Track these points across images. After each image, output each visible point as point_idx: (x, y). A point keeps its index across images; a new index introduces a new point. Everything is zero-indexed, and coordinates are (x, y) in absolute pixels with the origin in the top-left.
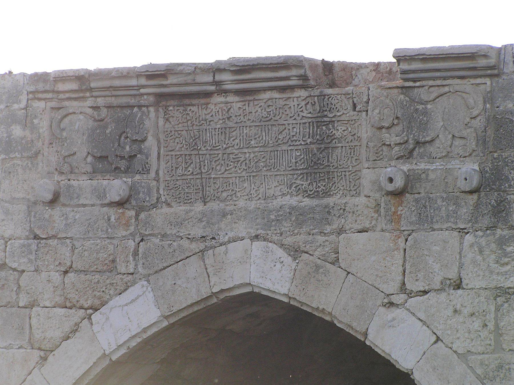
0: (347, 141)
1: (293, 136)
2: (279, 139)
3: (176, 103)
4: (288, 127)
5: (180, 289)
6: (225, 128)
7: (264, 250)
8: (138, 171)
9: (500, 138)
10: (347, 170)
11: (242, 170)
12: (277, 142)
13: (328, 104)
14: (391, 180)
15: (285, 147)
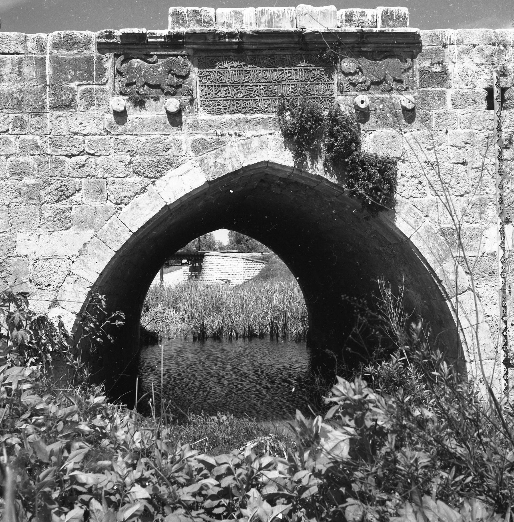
1: (289, 77)
5: (219, 165)
14: (362, 102)
15: (284, 83)
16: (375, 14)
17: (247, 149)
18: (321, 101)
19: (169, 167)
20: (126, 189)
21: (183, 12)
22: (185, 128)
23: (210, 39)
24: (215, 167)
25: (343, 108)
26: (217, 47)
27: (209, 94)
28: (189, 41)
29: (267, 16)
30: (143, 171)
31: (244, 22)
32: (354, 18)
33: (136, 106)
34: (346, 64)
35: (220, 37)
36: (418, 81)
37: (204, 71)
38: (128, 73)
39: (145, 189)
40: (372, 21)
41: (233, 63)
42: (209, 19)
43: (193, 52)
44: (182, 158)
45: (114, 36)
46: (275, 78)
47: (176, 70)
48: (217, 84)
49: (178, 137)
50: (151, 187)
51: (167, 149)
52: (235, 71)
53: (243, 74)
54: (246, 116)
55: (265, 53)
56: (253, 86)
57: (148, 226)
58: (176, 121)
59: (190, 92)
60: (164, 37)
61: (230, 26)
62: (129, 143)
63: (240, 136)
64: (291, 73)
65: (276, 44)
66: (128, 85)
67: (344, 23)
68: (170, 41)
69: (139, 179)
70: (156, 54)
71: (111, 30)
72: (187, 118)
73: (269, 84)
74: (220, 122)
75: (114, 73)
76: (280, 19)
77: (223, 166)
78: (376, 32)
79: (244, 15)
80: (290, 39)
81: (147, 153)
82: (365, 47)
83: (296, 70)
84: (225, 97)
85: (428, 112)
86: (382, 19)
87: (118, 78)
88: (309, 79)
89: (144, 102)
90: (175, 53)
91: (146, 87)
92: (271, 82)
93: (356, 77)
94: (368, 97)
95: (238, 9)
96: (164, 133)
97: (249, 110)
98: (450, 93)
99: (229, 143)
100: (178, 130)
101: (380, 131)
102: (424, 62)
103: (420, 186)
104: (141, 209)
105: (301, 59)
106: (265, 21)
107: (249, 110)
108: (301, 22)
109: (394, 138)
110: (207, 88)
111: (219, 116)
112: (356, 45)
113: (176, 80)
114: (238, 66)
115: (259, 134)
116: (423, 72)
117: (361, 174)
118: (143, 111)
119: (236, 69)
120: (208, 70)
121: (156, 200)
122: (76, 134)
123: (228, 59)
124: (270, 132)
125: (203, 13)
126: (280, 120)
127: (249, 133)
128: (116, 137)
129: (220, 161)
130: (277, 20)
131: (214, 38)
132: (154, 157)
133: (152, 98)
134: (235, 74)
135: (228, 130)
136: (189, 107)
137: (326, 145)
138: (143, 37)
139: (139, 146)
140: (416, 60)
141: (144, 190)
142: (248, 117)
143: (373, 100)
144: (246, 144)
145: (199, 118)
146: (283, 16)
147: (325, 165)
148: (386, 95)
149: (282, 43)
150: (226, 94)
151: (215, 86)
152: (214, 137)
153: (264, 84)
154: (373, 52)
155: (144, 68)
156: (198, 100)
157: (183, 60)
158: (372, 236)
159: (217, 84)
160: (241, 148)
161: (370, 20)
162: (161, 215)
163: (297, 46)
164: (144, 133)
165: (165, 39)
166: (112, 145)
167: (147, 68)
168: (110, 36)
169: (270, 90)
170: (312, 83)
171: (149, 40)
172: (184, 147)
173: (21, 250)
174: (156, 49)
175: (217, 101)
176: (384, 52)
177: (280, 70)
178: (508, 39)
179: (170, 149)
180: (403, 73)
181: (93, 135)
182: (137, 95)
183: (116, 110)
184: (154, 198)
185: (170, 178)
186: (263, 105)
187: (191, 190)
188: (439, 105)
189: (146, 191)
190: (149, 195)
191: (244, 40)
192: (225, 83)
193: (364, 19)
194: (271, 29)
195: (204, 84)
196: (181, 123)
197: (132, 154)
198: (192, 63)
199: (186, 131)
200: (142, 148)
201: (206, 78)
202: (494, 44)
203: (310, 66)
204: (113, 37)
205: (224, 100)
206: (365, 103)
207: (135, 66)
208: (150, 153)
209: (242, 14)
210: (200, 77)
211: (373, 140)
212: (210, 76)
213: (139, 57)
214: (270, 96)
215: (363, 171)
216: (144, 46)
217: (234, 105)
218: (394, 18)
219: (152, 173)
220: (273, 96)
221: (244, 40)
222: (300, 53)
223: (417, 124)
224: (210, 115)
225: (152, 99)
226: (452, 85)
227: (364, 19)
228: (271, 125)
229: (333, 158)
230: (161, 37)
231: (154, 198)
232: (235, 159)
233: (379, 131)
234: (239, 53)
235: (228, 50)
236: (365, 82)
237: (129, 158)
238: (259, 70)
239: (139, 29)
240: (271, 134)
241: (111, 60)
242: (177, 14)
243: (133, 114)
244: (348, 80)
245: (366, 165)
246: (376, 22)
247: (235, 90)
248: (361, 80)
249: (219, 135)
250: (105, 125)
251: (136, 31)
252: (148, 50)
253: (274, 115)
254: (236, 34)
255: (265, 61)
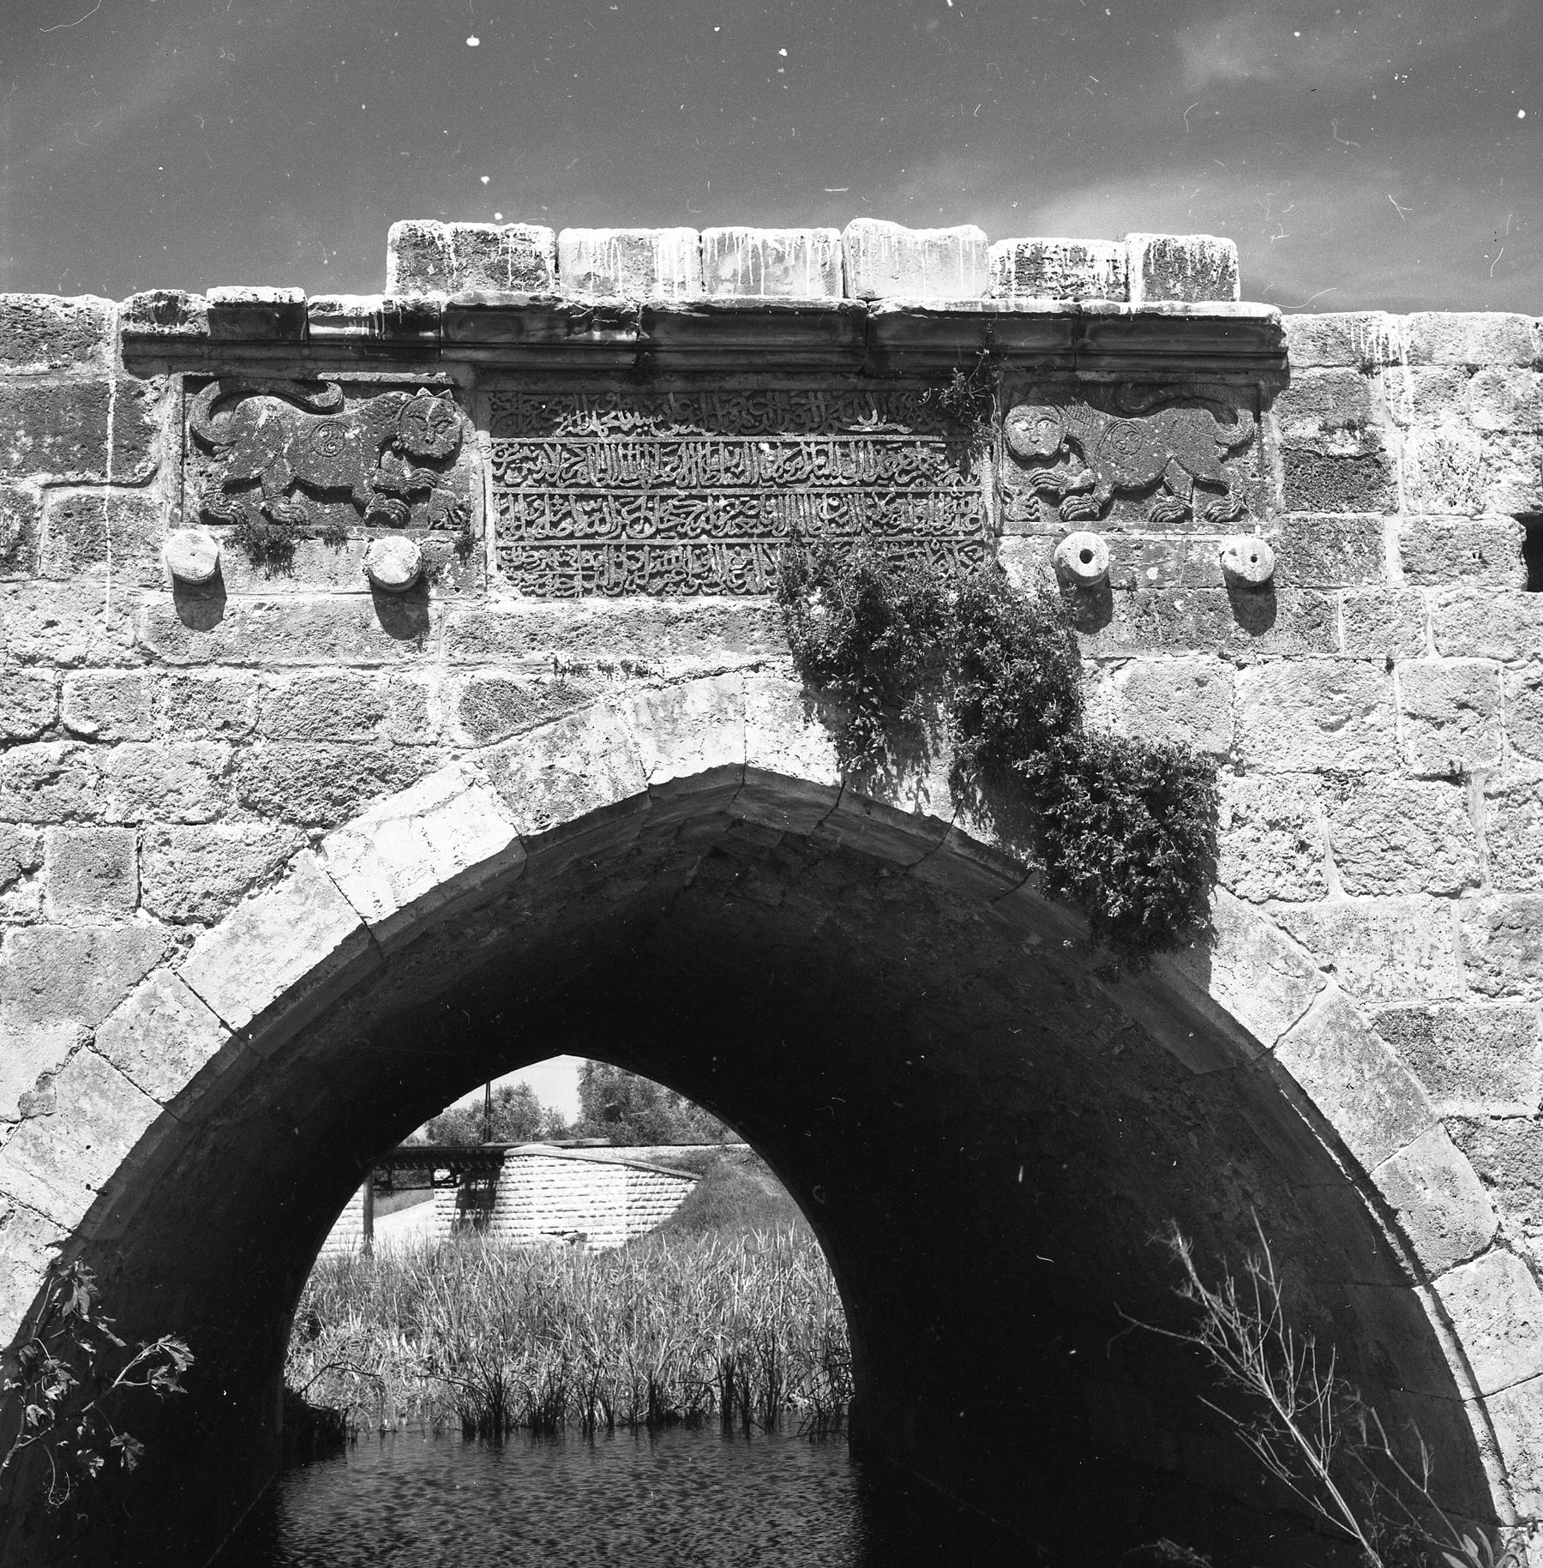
0: (947, 481)
1: (820, 467)
2: (786, 471)
3: (521, 388)
4: (805, 449)
5: (565, 778)
6: (651, 445)
7: (776, 695)
8: (435, 523)
9: (1298, 488)
10: (955, 538)
11: (699, 531)
12: (781, 477)
13: (897, 408)
14: (1086, 556)
15: (800, 489)
16: (1121, 258)
17: (667, 723)
18: (934, 552)
19: (376, 784)
20: (211, 864)
21: (441, 237)
22: (437, 644)
23: (537, 331)
24: (550, 784)
25: (1015, 576)
26: (560, 360)
27: (530, 524)
28: (459, 335)
29: (739, 255)
30: (276, 799)
31: (659, 275)
32: (1048, 269)
33: (257, 561)
34: (1024, 425)
35: (571, 325)
36: (1279, 487)
37: (511, 445)
38: (232, 444)
39: (285, 865)
40: (1112, 279)
41: (616, 418)
42: (532, 262)
43: (472, 376)
44: (426, 753)
45: (185, 314)
46: (770, 472)
47: (409, 439)
48: (558, 491)
49: (412, 676)
50: (306, 861)
51: (369, 718)
52: (625, 446)
53: (652, 456)
54: (665, 605)
55: (731, 383)
56: (690, 497)
57: (291, 1006)
58: (408, 618)
59: (460, 516)
60: (369, 320)
61: (605, 286)
62: (227, 697)
63: (641, 673)
64: (826, 454)
65: (772, 353)
66: (234, 487)
67: (1014, 285)
68: (390, 335)
69: (260, 828)
70: (338, 382)
71: (174, 292)
73: (748, 491)
74: (567, 622)
75: (183, 446)
76: (786, 270)
77: (578, 781)
78: (1128, 316)
79: (660, 250)
80: (824, 336)
81: (293, 734)
82: (1088, 369)
83: (845, 445)
84: (586, 536)
85: (1318, 593)
86: (1146, 275)
87: (195, 465)
88: (892, 478)
89: (291, 550)
90: (408, 376)
91: (298, 496)
92: (755, 486)
93: (1058, 470)
94: (1107, 541)
95: (636, 233)
96: (361, 660)
97: (677, 584)
98: (1394, 530)
99: (601, 698)
100: (413, 650)
101: (1151, 659)
102: (1298, 424)
103: (1302, 860)
104: (264, 940)
105: (862, 408)
106: (735, 274)
107: (677, 584)
108: (861, 278)
109: (1201, 683)
110: (522, 505)
111: (565, 604)
112: (1058, 361)
113: (408, 474)
114: (635, 427)
115: (714, 665)
116: (1296, 456)
117: (1089, 813)
118: (282, 583)
119: (630, 439)
120: (528, 441)
121: (325, 906)
122: (31, 660)
123: (602, 404)
124: (753, 660)
125: (512, 243)
126: (787, 617)
127: (676, 666)
128: (182, 673)
129: (569, 763)
130: (778, 270)
131: (551, 328)
132: (320, 746)
133: (318, 533)
134: (625, 457)
135: (597, 652)
136: (454, 570)
137: (955, 709)
138: (293, 314)
139: (266, 708)
140: (1272, 417)
141: (280, 868)
142: (673, 606)
143: (1122, 550)
144: (664, 703)
145: (493, 608)
146: (797, 258)
147: (955, 781)
148: (1174, 534)
149: (795, 348)
150: (591, 525)
151: (552, 497)
152: (548, 678)
153: (730, 491)
154: (1118, 384)
155: (295, 429)
156: (490, 545)
157: (435, 402)
158: (1117, 1051)
159: (558, 491)
160: (645, 718)
161: (1103, 277)
162: (343, 963)
163: (849, 361)
164: (284, 661)
165: (372, 327)
166: (166, 702)
167: (304, 427)
168: (171, 311)
169: (752, 512)
170: (903, 489)
171: (315, 330)
172: (433, 711)
174: (338, 364)
175: (558, 548)
176: (1154, 386)
177: (785, 445)
179: (380, 717)
180: (1223, 459)
181: (93, 665)
182: (262, 524)
183: (181, 573)
184: (317, 902)
185: (379, 824)
186: (724, 563)
187: (459, 870)
188: (1359, 573)
189: (286, 872)
190: (299, 890)
191: (659, 334)
192: (590, 485)
193: (1082, 272)
194: (756, 297)
195: (509, 490)
196: (425, 625)
197: (237, 736)
198: (471, 415)
199: (442, 655)
200: (275, 715)
201: (520, 469)
203: (896, 432)
204: (184, 317)
205: (584, 547)
206: (1094, 560)
207: (261, 422)
208: (307, 733)
209: (651, 248)
210: (498, 465)
211: (1127, 692)
212: (534, 460)
213: (279, 387)
214: (751, 536)
215: (1094, 800)
216: (292, 353)
217: (619, 565)
218: (1189, 272)
219: (312, 808)
220: (761, 535)
221: (659, 334)
222: (860, 385)
223: (1279, 639)
224: (533, 598)
225: (321, 540)
226: (1402, 502)
227: (1082, 272)
228: (757, 635)
229: (982, 757)
230: (358, 320)
231: (317, 902)
232: (624, 758)
233: (1146, 662)
234: (638, 383)
235: (602, 373)
236: (1091, 489)
237: (225, 749)
238: (712, 444)
239: (279, 291)
240: (755, 668)
241: (172, 399)
242: (416, 245)
244: (1033, 482)
245: (1101, 778)
246: (1126, 285)
247: (624, 511)
248: (1076, 482)
249: (564, 670)
250: (139, 630)
251: (267, 294)
252: (310, 365)
253: (764, 603)
254: (630, 316)
255: (735, 411)
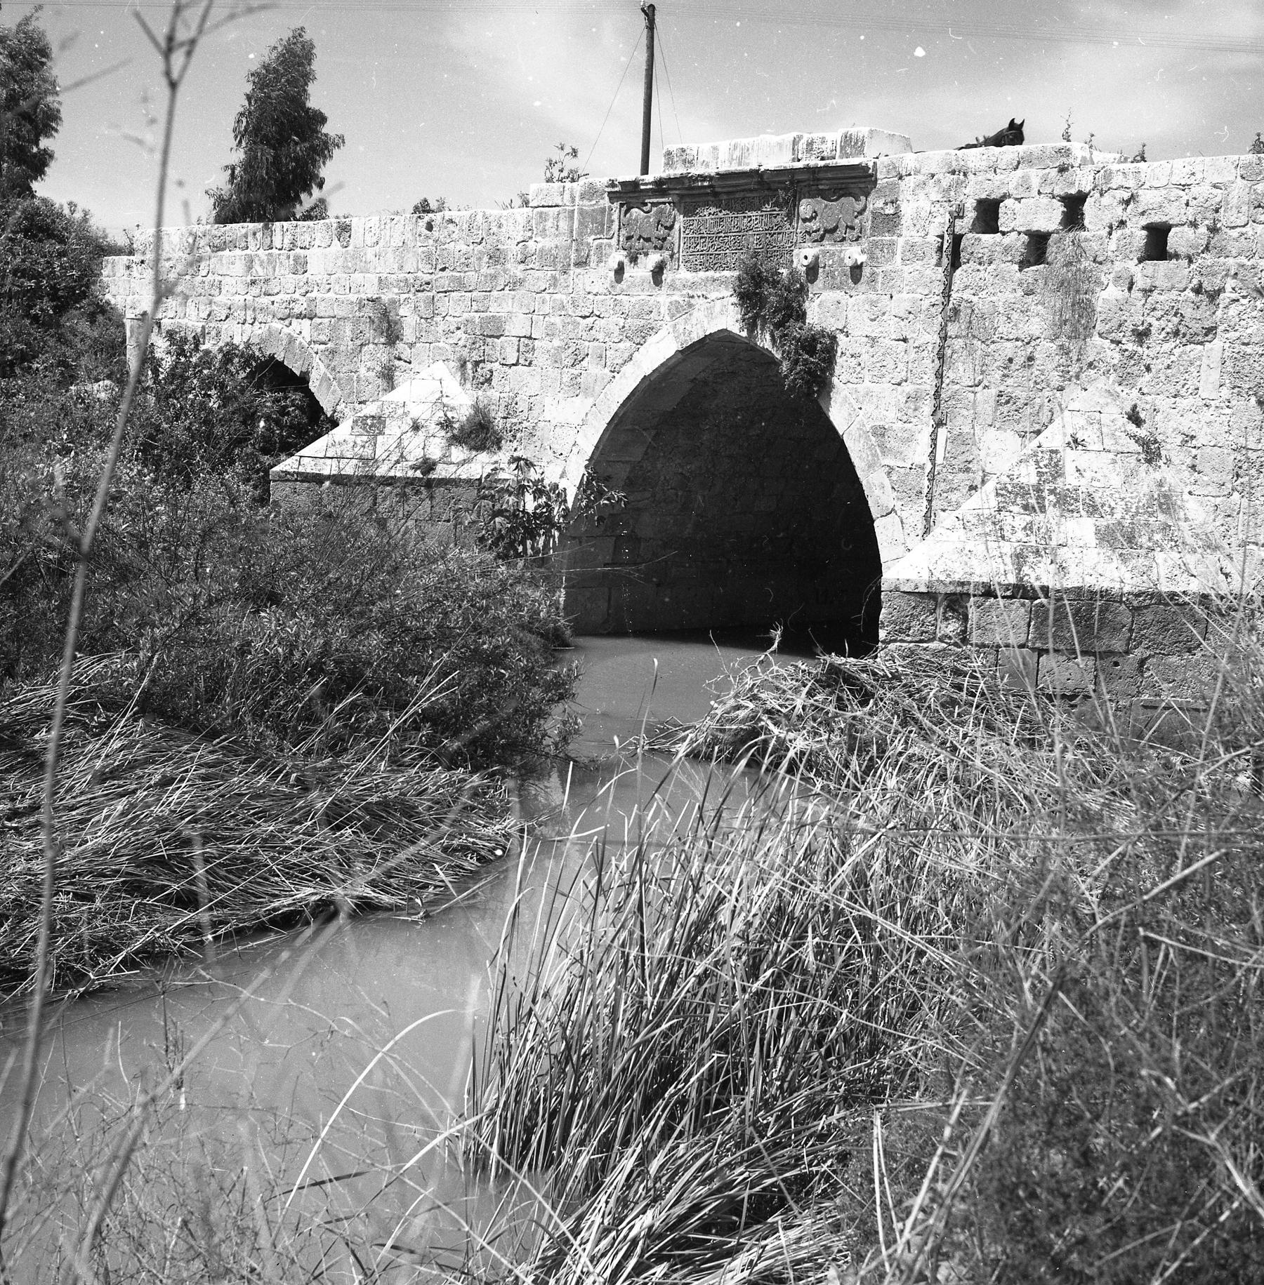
17: (710, 314)
55: (737, 196)
69: (628, 344)
72: (667, 276)
98: (901, 242)
103: (859, 369)
116: (875, 215)
127: (713, 296)
148: (837, 247)
173: (547, 416)
178: (971, 165)
202: (953, 173)
223: (862, 286)
226: (904, 232)
243: (629, 271)
